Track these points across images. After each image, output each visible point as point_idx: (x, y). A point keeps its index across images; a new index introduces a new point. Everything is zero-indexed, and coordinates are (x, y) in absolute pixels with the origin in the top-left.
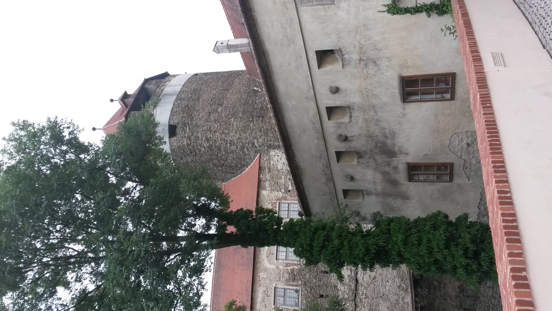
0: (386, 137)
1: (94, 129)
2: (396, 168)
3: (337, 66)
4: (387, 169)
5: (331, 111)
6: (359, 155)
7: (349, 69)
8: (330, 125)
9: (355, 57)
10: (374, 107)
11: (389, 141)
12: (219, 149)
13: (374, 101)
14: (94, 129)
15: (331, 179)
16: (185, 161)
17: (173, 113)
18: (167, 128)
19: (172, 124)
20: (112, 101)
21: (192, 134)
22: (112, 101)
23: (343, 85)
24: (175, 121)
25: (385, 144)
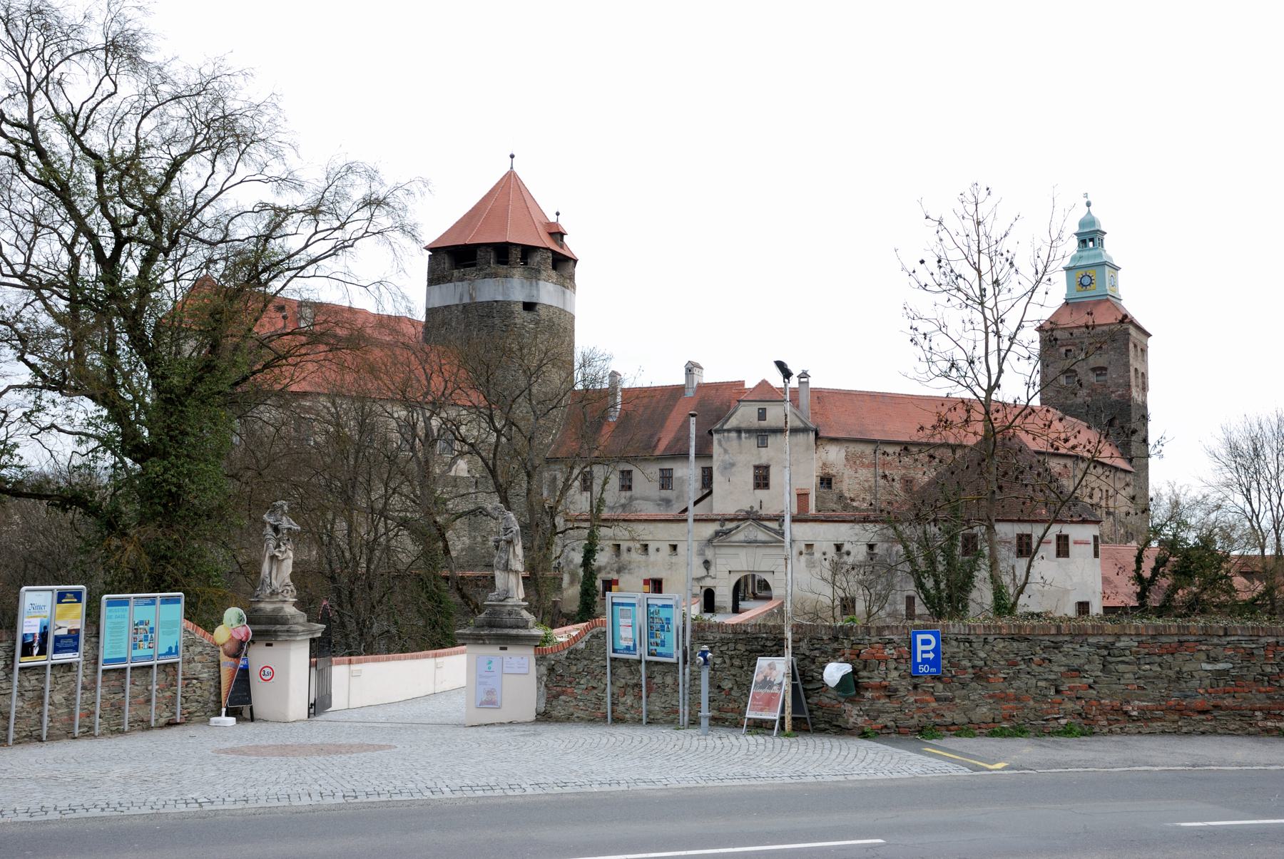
0: (629, 570)
1: (512, 156)
2: (609, 573)
3: (669, 552)
4: (608, 569)
5: (646, 546)
7: (668, 558)
9: (673, 561)
10: (647, 566)
11: (626, 571)
13: (650, 566)
14: (512, 156)
16: (495, 315)
18: (534, 300)
19: (538, 307)
20: (558, 214)
21: (526, 331)
22: (558, 214)
23: (660, 554)
24: (543, 312)
25: (625, 569)
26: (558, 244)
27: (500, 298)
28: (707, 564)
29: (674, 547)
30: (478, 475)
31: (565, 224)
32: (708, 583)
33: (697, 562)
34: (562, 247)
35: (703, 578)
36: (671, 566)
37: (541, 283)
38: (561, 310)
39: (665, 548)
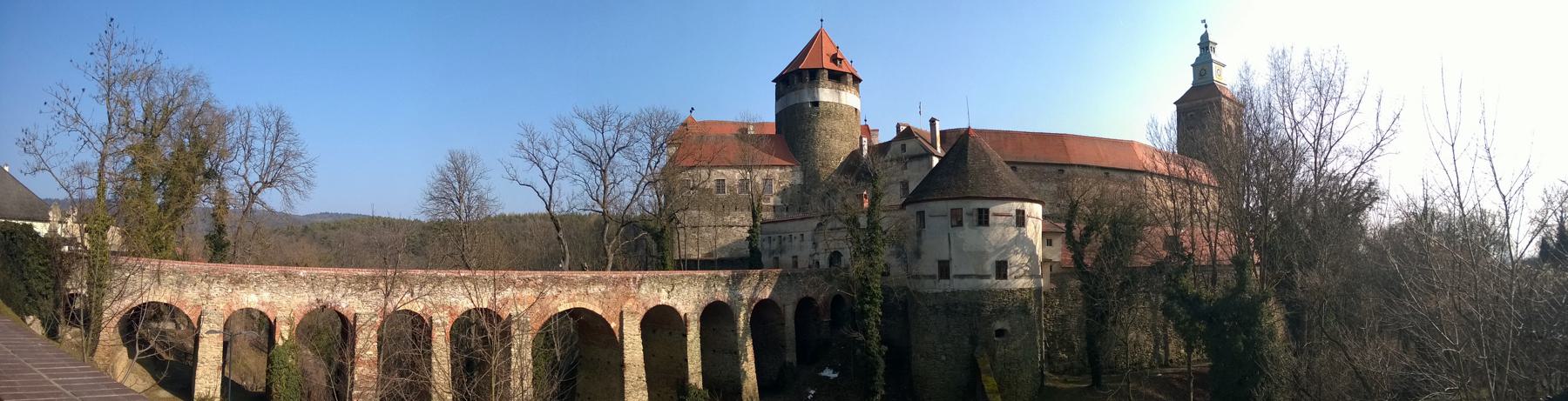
1: (822, 20)
6: (780, 243)
8: (787, 235)
12: (804, 137)
14: (822, 20)
15: (774, 233)
17: (825, 103)
24: (821, 106)
26: (836, 64)
27: (798, 102)
28: (815, 244)
29: (802, 235)
30: (787, 204)
31: (844, 53)
32: (816, 257)
33: (810, 244)
34: (840, 67)
35: (814, 255)
36: (801, 248)
37: (820, 89)
38: (836, 104)
39: (798, 235)
